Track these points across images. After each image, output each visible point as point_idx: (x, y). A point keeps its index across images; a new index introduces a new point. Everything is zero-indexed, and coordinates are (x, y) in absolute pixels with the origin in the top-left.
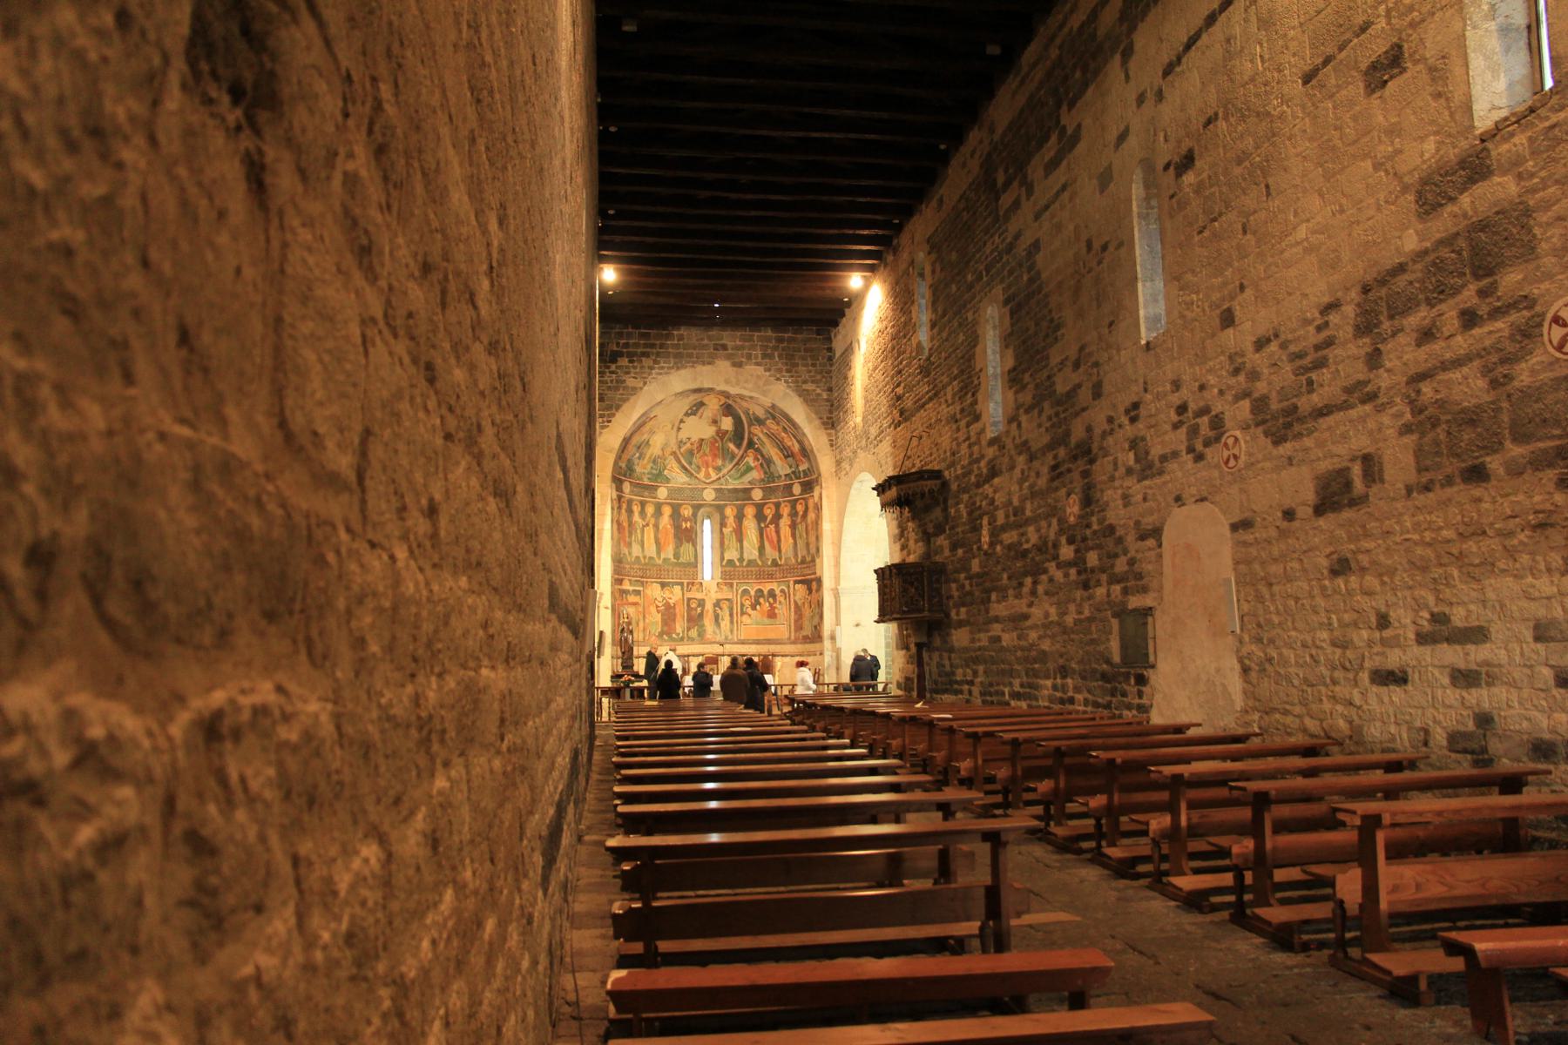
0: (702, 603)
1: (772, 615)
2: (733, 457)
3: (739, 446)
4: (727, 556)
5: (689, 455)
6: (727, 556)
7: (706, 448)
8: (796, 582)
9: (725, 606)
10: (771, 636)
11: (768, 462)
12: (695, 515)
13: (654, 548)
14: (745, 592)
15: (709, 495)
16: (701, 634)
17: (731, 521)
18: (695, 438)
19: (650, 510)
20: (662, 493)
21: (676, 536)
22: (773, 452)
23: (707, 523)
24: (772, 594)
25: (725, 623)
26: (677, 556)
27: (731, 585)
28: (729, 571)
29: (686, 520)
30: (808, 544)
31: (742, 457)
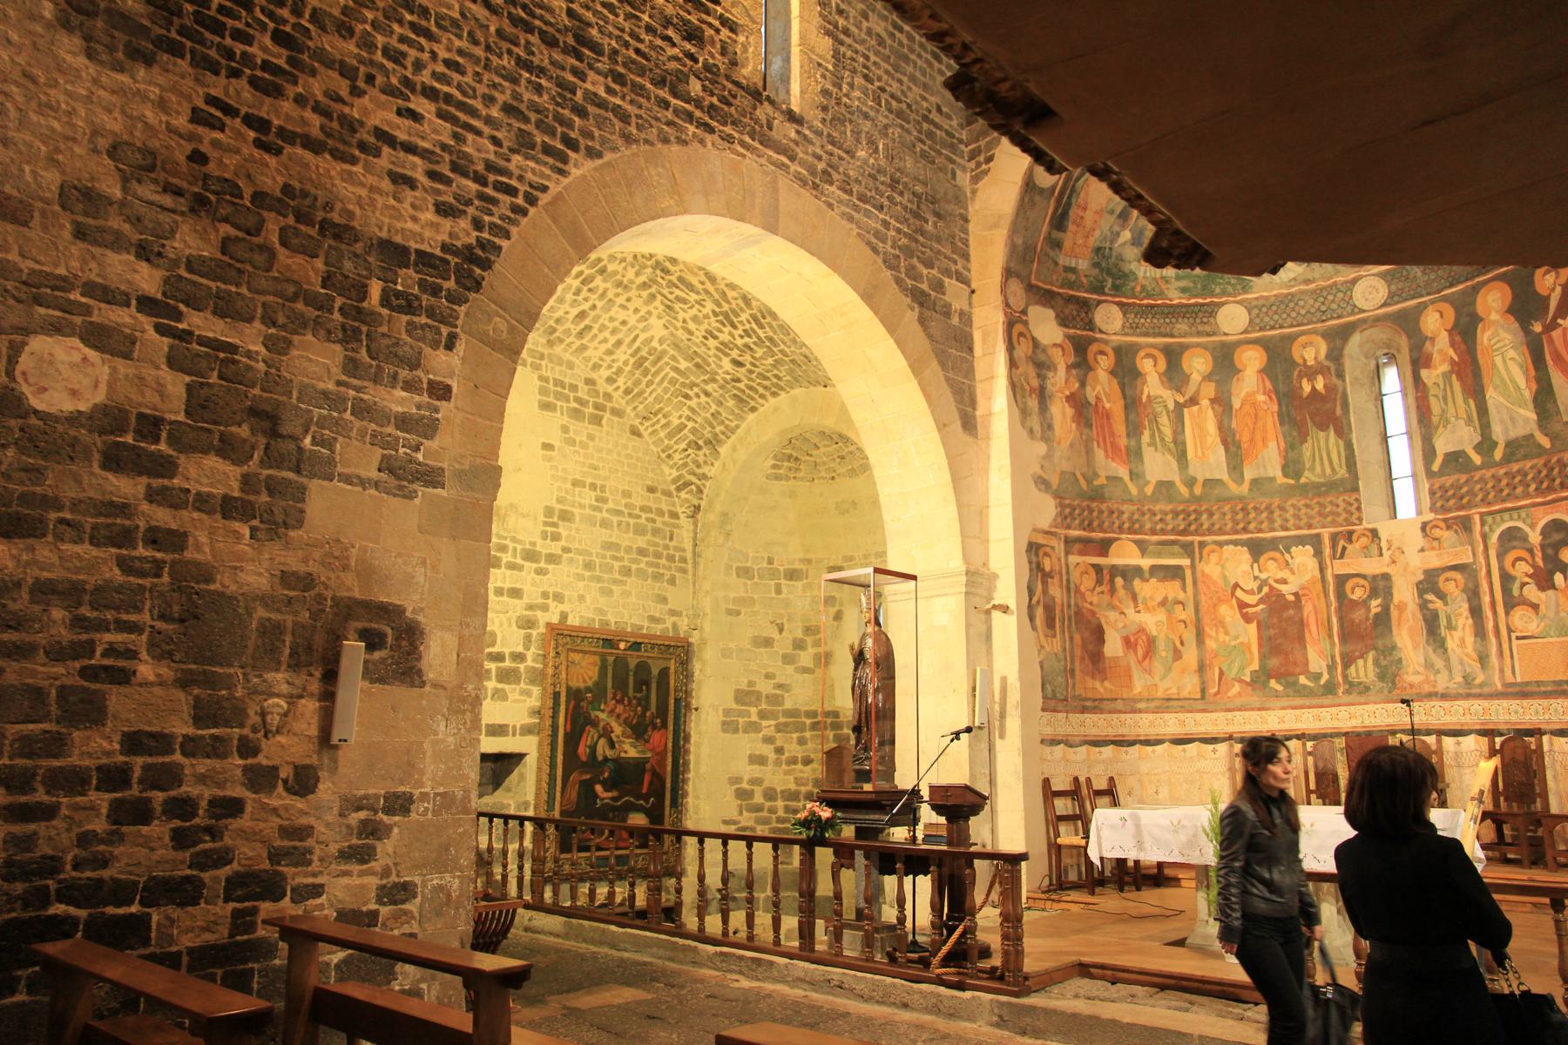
0: (1381, 585)
4: (1442, 446)
6: (1442, 446)
9: (1453, 586)
12: (1336, 356)
14: (1511, 537)
16: (1389, 673)
17: (1442, 348)
19: (1197, 365)
21: (1284, 418)
23: (1391, 379)
25: (1460, 638)
26: (1291, 467)
27: (1465, 525)
28: (1454, 487)
29: (1311, 374)
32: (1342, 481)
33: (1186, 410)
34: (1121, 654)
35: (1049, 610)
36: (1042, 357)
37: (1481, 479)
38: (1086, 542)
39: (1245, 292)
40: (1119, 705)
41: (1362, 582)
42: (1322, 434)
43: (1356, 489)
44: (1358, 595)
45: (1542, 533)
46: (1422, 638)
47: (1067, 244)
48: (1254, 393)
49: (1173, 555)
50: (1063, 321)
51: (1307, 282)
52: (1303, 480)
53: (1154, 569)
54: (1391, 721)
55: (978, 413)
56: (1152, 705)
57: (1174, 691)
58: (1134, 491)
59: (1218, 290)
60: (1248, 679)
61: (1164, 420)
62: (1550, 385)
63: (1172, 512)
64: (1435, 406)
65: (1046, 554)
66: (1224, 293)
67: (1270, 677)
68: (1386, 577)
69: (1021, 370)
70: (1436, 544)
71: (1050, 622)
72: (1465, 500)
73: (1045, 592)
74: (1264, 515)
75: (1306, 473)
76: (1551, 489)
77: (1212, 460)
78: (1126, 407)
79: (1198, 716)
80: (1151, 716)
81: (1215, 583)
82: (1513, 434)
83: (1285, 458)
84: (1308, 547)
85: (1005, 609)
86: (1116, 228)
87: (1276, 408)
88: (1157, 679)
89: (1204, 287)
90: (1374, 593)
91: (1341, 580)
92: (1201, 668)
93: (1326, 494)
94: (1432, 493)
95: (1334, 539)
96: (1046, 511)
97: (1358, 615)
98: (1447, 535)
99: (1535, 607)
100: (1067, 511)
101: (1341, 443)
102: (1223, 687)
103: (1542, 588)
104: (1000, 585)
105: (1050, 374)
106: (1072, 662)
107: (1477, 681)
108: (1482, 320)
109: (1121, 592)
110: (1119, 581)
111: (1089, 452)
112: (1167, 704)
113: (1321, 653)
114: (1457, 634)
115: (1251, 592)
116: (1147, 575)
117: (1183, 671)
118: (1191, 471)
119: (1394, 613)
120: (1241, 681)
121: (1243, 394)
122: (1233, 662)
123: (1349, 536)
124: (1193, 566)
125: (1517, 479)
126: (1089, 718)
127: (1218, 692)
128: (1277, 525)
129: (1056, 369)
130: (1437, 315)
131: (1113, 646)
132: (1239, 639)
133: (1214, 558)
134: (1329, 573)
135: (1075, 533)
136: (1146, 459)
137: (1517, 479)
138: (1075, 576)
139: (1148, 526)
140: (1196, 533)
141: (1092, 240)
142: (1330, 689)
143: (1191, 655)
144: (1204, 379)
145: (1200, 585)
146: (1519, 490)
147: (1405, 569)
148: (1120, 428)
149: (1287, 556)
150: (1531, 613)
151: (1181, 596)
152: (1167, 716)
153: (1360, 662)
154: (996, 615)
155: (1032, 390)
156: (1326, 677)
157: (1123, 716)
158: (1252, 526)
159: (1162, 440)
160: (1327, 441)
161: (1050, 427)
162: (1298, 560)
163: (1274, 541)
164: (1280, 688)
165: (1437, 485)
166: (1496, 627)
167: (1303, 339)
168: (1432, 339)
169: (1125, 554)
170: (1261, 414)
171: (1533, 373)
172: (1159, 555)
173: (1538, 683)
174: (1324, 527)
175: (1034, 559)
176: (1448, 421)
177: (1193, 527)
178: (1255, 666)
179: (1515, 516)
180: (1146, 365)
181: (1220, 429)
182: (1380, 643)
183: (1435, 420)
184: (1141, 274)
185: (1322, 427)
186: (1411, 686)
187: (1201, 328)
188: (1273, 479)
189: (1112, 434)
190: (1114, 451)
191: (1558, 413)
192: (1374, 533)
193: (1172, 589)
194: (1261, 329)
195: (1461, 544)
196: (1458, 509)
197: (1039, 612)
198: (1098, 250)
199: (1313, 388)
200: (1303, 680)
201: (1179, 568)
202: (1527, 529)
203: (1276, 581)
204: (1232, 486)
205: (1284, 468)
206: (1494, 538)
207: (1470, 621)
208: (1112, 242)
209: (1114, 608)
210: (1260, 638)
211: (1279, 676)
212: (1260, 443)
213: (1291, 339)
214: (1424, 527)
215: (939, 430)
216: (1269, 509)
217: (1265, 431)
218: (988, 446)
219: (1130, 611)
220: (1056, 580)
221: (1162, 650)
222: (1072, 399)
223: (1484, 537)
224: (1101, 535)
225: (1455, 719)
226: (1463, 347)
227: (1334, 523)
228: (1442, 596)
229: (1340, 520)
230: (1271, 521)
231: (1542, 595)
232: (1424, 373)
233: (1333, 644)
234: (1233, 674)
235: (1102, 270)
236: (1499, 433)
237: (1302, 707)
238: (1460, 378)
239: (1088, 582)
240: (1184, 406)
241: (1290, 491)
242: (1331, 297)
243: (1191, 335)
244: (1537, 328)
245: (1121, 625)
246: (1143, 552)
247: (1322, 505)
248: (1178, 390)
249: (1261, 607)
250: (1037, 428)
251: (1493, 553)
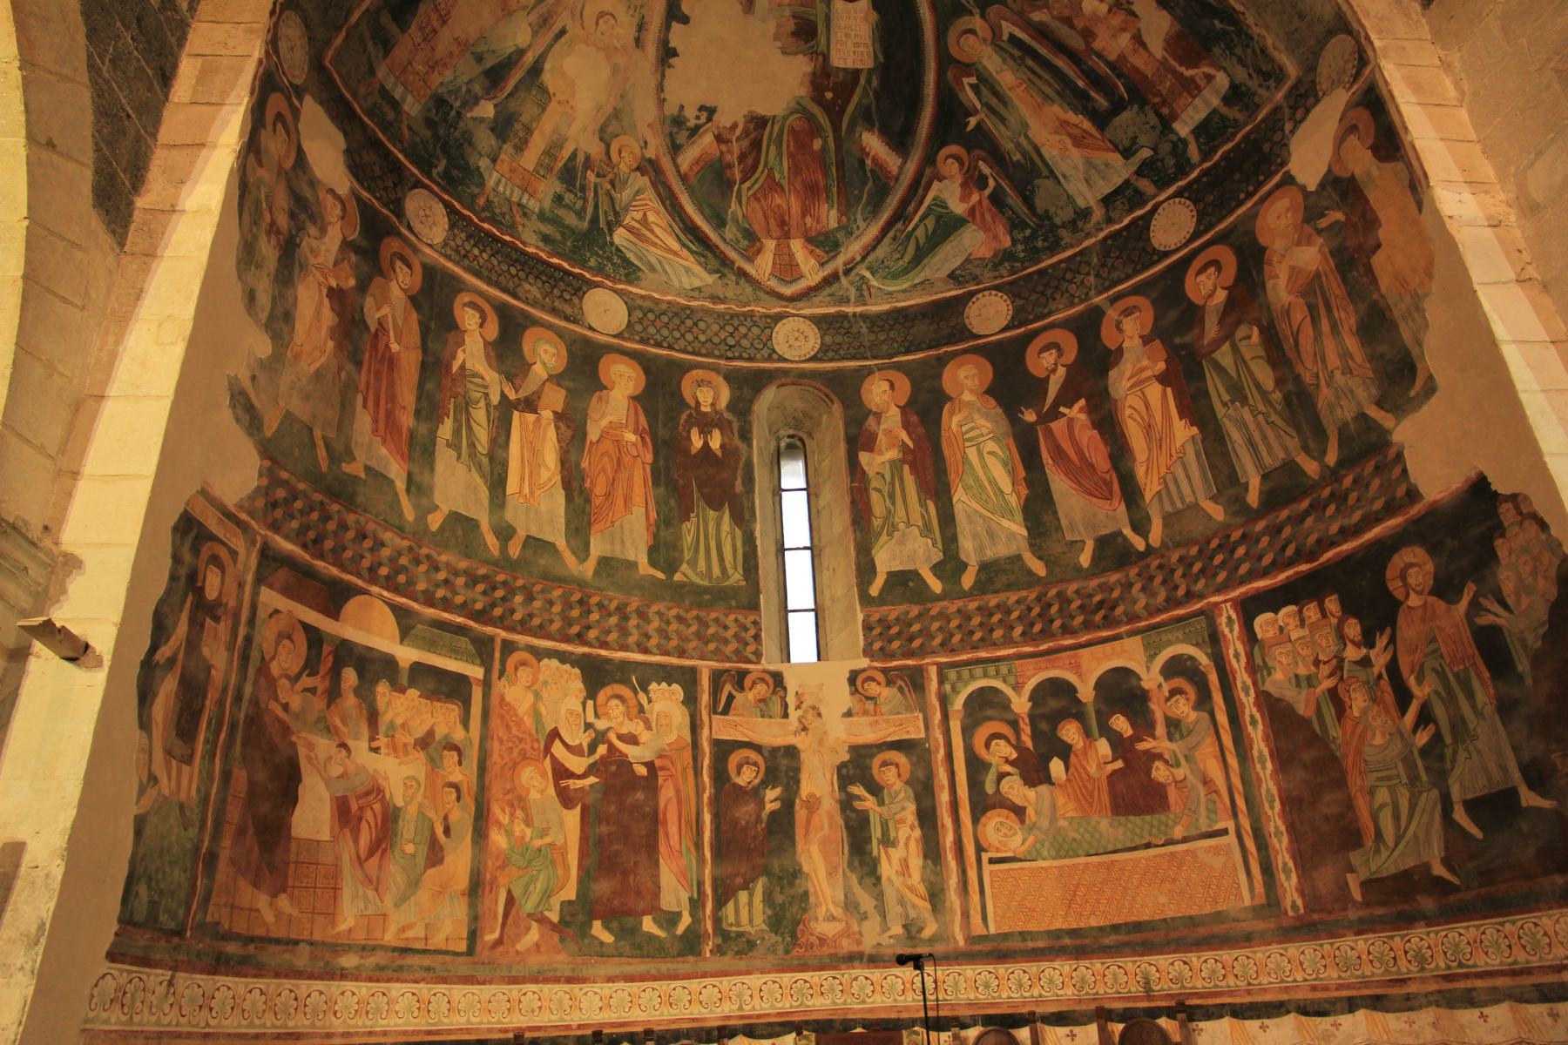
0: (782, 766)
1: (1136, 793)
2: (882, 192)
3: (900, 141)
4: (886, 559)
5: (717, 184)
6: (886, 559)
7: (777, 161)
8: (1249, 609)
9: (893, 774)
10: (1154, 904)
11: (1026, 174)
12: (741, 408)
13: (554, 504)
14: (984, 704)
15: (796, 340)
16: (788, 918)
17: (891, 427)
18: (731, 114)
19: (545, 355)
20: (605, 311)
21: (659, 475)
22: (1042, 126)
23: (793, 474)
24: (1121, 692)
25: (902, 861)
26: (663, 552)
27: (915, 681)
29: (706, 424)
30: (1299, 405)
31: (918, 186)
32: (735, 589)
33: (516, 414)
34: (325, 835)
35: (192, 691)
36: (307, 192)
37: (944, 616)
38: (308, 573)
39: (630, 283)
40: (301, 958)
41: (754, 756)
42: (712, 514)
43: (754, 606)
44: (746, 777)
45: (1031, 698)
46: (842, 857)
47: (400, 53)
48: (620, 426)
49: (455, 653)
50: (356, 168)
51: (715, 299)
52: (678, 577)
53: (418, 670)
54: (786, 1005)
55: (140, 203)
56: (371, 961)
57: (417, 932)
58: (409, 515)
59: (592, 263)
60: (555, 918)
61: (479, 414)
62: (1048, 490)
63: (466, 573)
64: (878, 504)
65: (215, 560)
66: (599, 270)
67: (593, 916)
68: (791, 752)
69: (262, 173)
70: (870, 706)
71: (186, 722)
72: (916, 644)
73: (192, 645)
74: (613, 620)
75: (684, 567)
76: (1046, 634)
77: (543, 508)
78: (424, 366)
79: (458, 991)
80: (363, 989)
81: (520, 722)
82: (990, 554)
83: (655, 536)
84: (676, 687)
85: (76, 651)
86: (477, 88)
87: (649, 458)
88: (389, 901)
89: (576, 249)
90: (770, 778)
91: (723, 749)
92: (476, 887)
93: (709, 606)
94: (867, 627)
95: (717, 678)
96: (238, 475)
97: (744, 812)
98: (886, 693)
99: (1019, 812)
100: (281, 493)
101: (738, 532)
102: (510, 931)
103: (1030, 782)
104: (77, 586)
105: (313, 231)
106: (217, 835)
107: (926, 934)
108: (950, 398)
109: (350, 701)
110: (350, 676)
111: (346, 408)
112: (402, 962)
113: (683, 877)
114: (896, 854)
115: (575, 750)
116: (404, 680)
117: (441, 890)
118: (509, 515)
119: (800, 813)
120: (542, 920)
121: (604, 423)
122: (533, 880)
123: (740, 679)
124: (487, 684)
125: (998, 617)
126: (228, 986)
127: (499, 942)
128: (631, 640)
129: (323, 231)
130: (886, 386)
131: (312, 817)
132: (547, 832)
133: (524, 675)
134: (706, 732)
135: (288, 546)
136: (440, 466)
137: (998, 617)
138: (266, 634)
139: (421, 586)
140: (501, 622)
141: (435, 80)
142: (690, 944)
143: (459, 859)
144: (551, 378)
145: (495, 722)
146: (998, 634)
147: (821, 742)
148: (408, 396)
149: (642, 697)
150: (1012, 820)
151: (459, 735)
152: (396, 989)
153: (743, 896)
154: (44, 663)
155: (273, 229)
156: (686, 920)
157: (304, 986)
158: (592, 634)
159: (472, 445)
160: (718, 525)
161: (288, 317)
162: (658, 707)
163: (625, 666)
164: (608, 938)
165: (875, 617)
166: (959, 843)
167: (698, 374)
168: (878, 415)
169: (371, 626)
170: (626, 460)
171: (1022, 473)
172: (432, 646)
173: (1024, 935)
174: (701, 658)
175: (187, 556)
176: (895, 528)
177: (498, 611)
178: (570, 893)
179: (992, 670)
180: (469, 319)
181: (564, 462)
182: (775, 864)
183: (876, 523)
184: (491, 183)
185: (718, 507)
186: (822, 941)
187: (557, 303)
188: (633, 565)
189: (392, 398)
190: (388, 427)
191: (1059, 527)
192: (778, 680)
193: (443, 718)
194: (642, 341)
195: (908, 709)
196: (909, 654)
197: (168, 687)
198: (440, 102)
199: (706, 444)
200: (648, 925)
201: (463, 680)
202: (1008, 691)
203: (620, 737)
204: (570, 559)
205: (653, 551)
206: (958, 703)
207: (917, 833)
208: (464, 104)
209: (329, 730)
210: (584, 839)
211: (610, 916)
212: (620, 502)
213: (684, 368)
214: (853, 678)
215: (31, 138)
216: (621, 610)
217: (630, 488)
218: (145, 271)
219: (360, 746)
220: (223, 628)
221: (409, 844)
222: (336, 295)
223: (944, 701)
224: (334, 571)
225: (889, 1002)
226: (921, 430)
227: (718, 655)
228: (875, 789)
229: (728, 650)
230: (624, 632)
231: (1031, 793)
232: (864, 457)
233: (701, 860)
234: (529, 907)
235: (436, 136)
236: (968, 548)
237: (642, 978)
238: (915, 470)
239: (287, 659)
240: (515, 405)
241: (654, 591)
242: (743, 330)
243: (543, 308)
244: (1030, 416)
245: (336, 770)
246: (405, 634)
247: (702, 622)
248: (510, 378)
249: (592, 780)
250: (264, 299)
251: (956, 726)
